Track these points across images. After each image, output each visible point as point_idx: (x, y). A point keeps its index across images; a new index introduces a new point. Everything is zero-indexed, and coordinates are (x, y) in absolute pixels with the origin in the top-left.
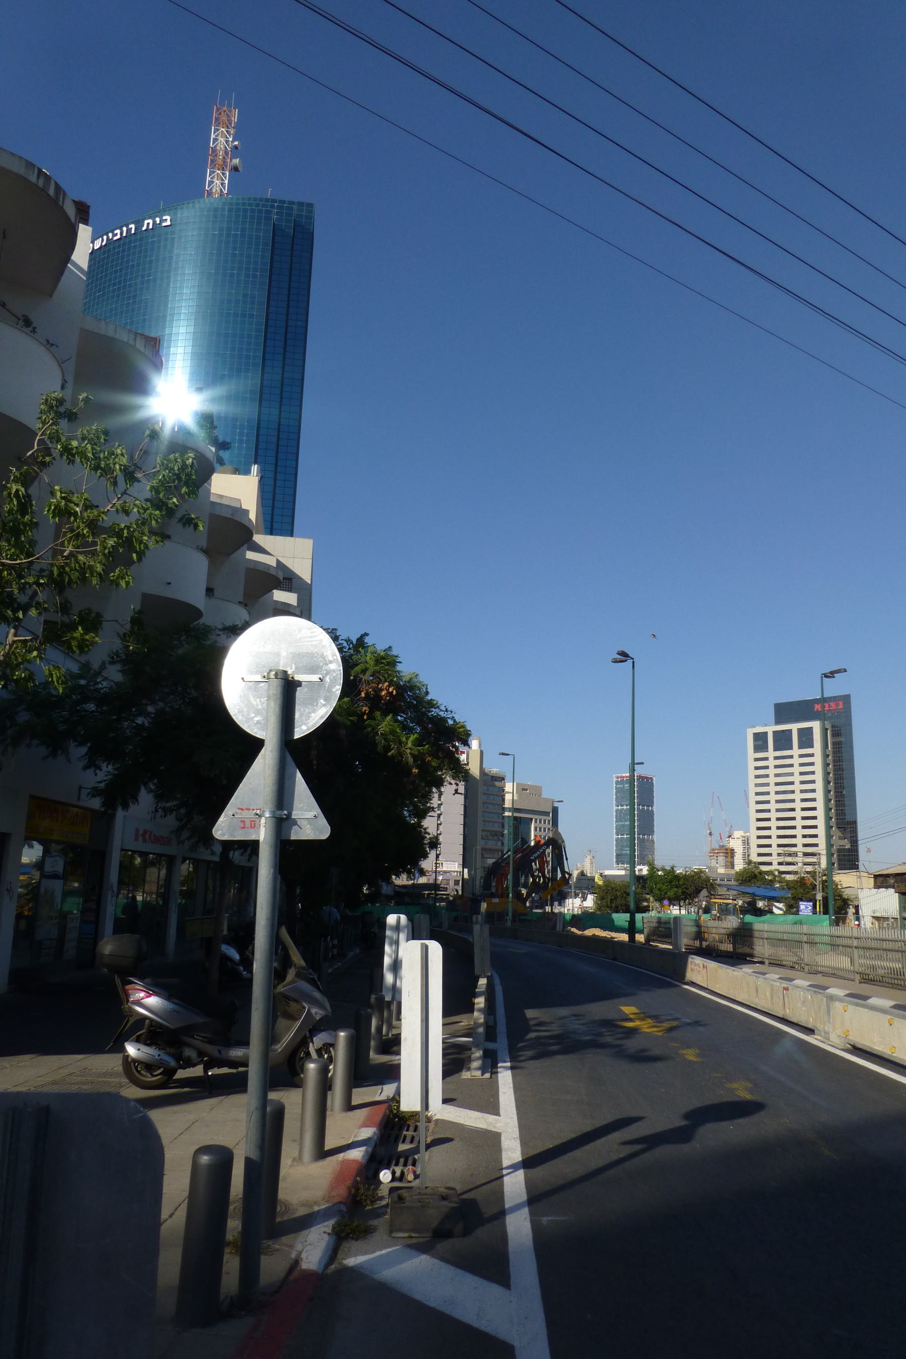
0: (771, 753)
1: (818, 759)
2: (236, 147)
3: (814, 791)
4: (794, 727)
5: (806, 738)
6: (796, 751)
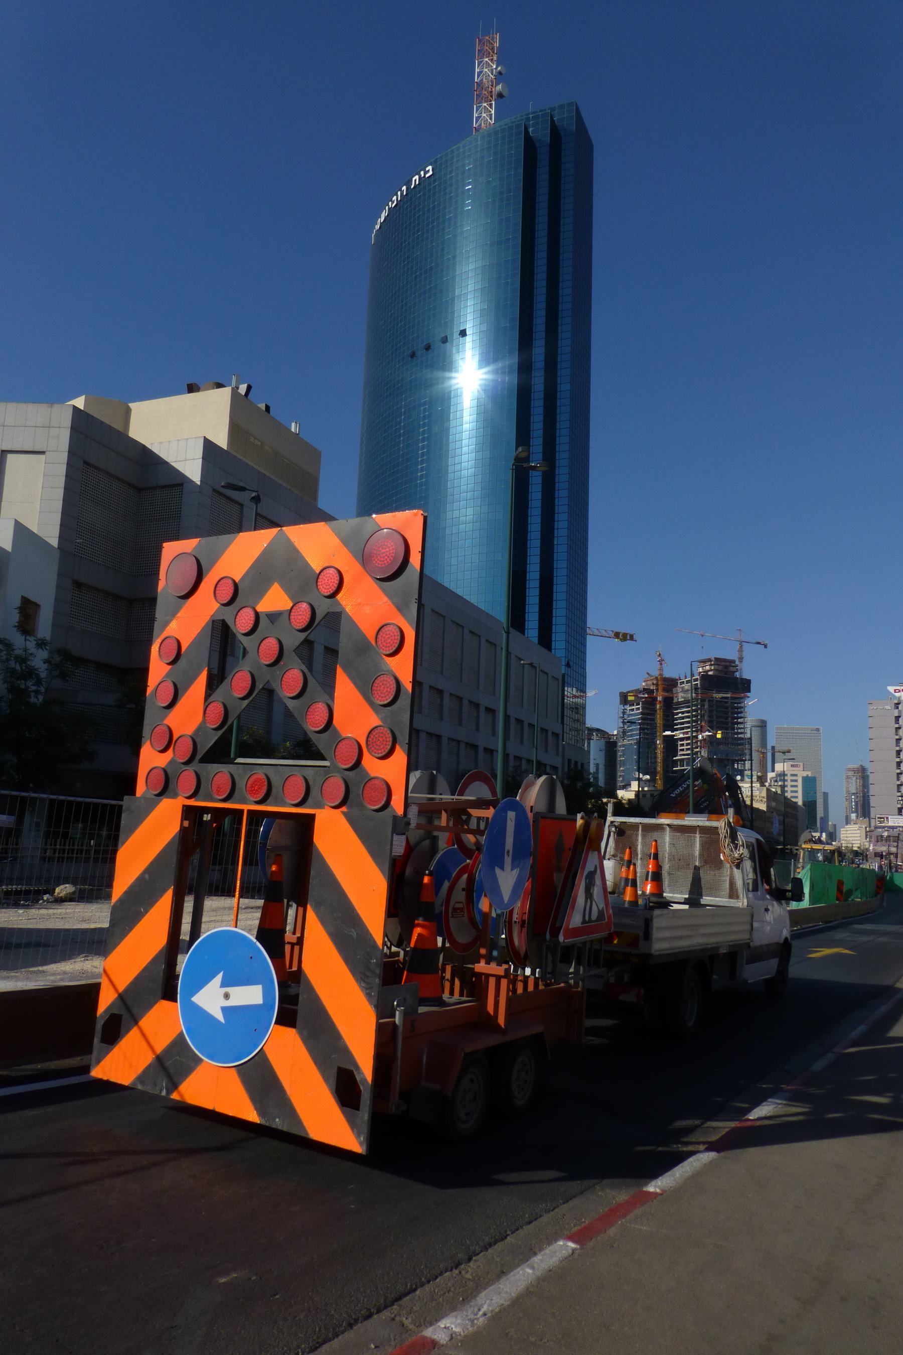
2: (500, 73)
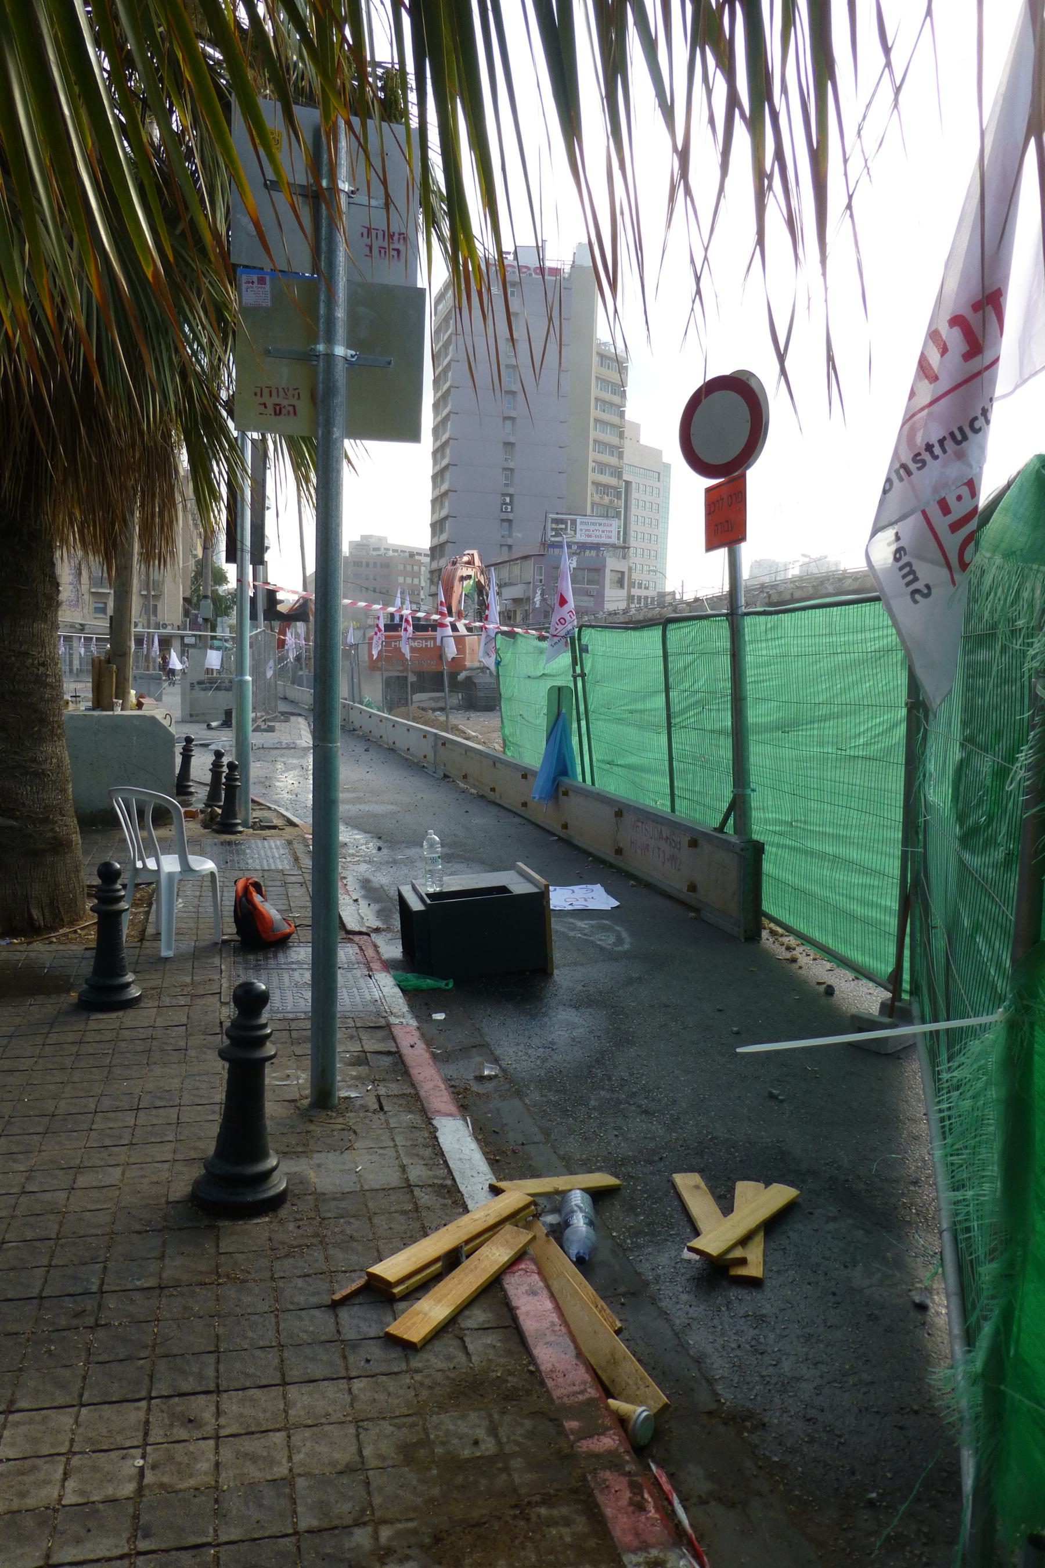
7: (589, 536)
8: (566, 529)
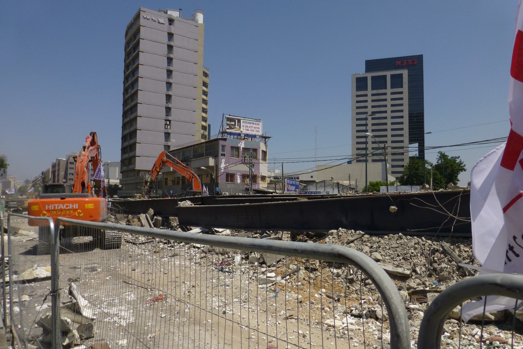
0: (370, 91)
1: (405, 95)
3: (402, 117)
4: (388, 74)
5: (397, 81)
6: (389, 90)
7: (248, 130)
8: (235, 125)
